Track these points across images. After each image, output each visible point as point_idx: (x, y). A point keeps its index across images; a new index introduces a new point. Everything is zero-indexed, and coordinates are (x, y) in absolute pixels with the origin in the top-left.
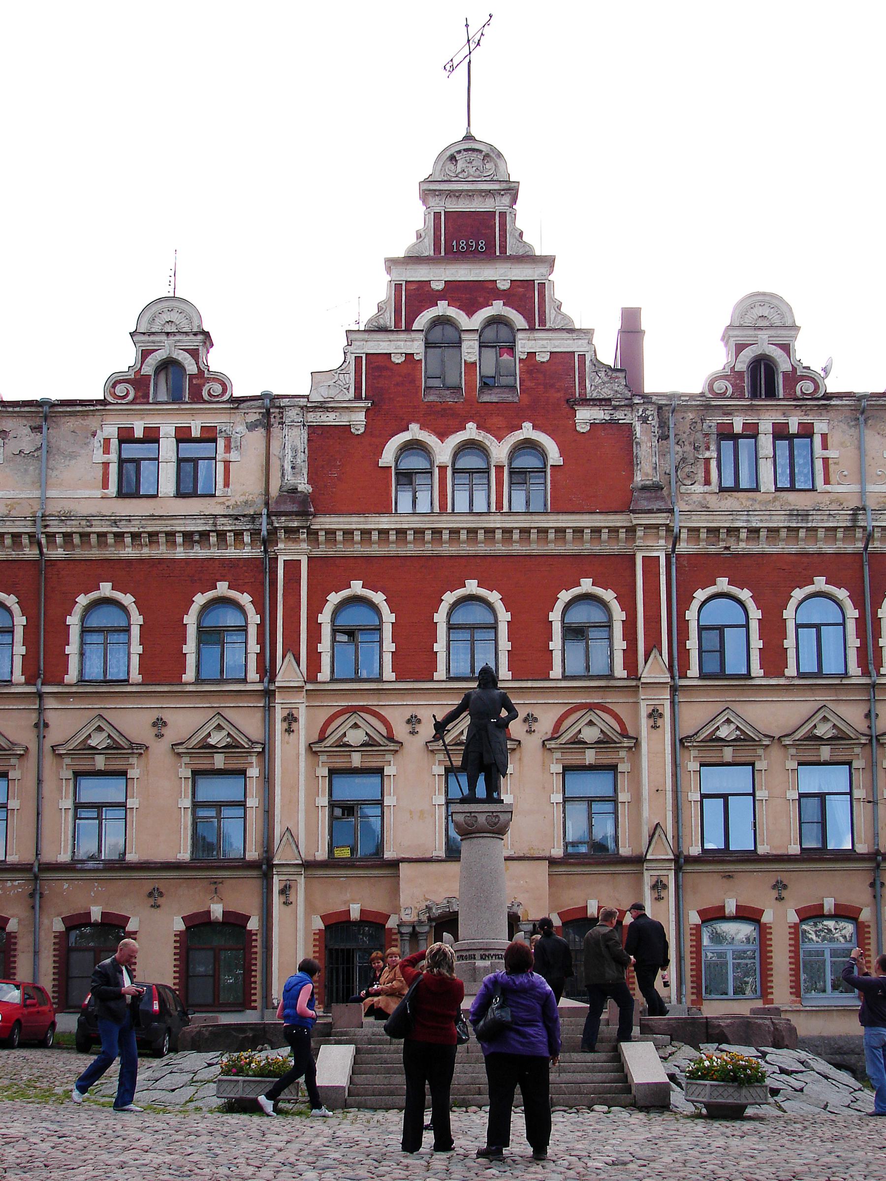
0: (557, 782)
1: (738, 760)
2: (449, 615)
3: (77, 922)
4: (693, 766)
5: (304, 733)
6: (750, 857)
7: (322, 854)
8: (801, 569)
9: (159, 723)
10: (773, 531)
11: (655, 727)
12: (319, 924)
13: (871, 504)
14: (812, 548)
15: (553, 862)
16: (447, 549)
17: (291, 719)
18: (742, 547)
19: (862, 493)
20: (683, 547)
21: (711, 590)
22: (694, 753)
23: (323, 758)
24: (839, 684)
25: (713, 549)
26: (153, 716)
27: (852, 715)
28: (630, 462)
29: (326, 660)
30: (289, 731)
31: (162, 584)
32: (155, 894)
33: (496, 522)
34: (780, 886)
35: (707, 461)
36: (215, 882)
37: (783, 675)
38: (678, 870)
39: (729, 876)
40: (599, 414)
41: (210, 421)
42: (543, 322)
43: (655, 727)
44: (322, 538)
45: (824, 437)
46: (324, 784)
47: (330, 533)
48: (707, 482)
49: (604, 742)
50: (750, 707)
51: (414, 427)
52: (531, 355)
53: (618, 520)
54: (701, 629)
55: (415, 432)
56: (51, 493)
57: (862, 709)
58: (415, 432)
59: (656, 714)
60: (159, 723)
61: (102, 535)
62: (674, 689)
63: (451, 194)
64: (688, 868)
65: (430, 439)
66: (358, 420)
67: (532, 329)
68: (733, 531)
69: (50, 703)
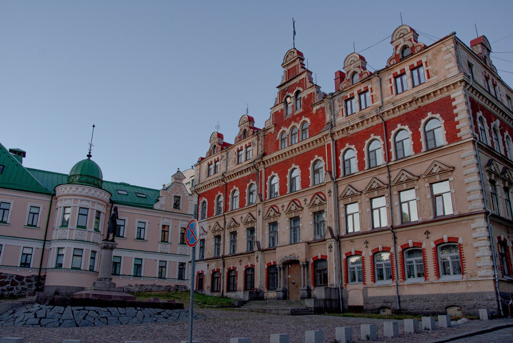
0: (312, 218)
1: (353, 201)
8: (366, 134)
10: (357, 124)
11: (330, 196)
12: (266, 267)
16: (288, 157)
17: (259, 212)
18: (351, 132)
19: (382, 102)
20: (337, 138)
23: (267, 220)
24: (379, 168)
25: (344, 136)
26: (240, 216)
27: (384, 178)
28: (324, 118)
31: (242, 184)
33: (295, 146)
35: (342, 109)
37: (363, 170)
40: (318, 107)
41: (250, 141)
42: (306, 87)
44: (266, 163)
45: (371, 89)
46: (267, 228)
47: (267, 161)
48: (343, 116)
49: (320, 204)
51: (282, 127)
52: (304, 97)
53: (320, 136)
55: (283, 129)
57: (387, 175)
58: (283, 129)
59: (330, 192)
60: (242, 218)
61: (233, 175)
63: (288, 65)
65: (285, 129)
66: (272, 130)
67: (304, 90)
68: (347, 128)
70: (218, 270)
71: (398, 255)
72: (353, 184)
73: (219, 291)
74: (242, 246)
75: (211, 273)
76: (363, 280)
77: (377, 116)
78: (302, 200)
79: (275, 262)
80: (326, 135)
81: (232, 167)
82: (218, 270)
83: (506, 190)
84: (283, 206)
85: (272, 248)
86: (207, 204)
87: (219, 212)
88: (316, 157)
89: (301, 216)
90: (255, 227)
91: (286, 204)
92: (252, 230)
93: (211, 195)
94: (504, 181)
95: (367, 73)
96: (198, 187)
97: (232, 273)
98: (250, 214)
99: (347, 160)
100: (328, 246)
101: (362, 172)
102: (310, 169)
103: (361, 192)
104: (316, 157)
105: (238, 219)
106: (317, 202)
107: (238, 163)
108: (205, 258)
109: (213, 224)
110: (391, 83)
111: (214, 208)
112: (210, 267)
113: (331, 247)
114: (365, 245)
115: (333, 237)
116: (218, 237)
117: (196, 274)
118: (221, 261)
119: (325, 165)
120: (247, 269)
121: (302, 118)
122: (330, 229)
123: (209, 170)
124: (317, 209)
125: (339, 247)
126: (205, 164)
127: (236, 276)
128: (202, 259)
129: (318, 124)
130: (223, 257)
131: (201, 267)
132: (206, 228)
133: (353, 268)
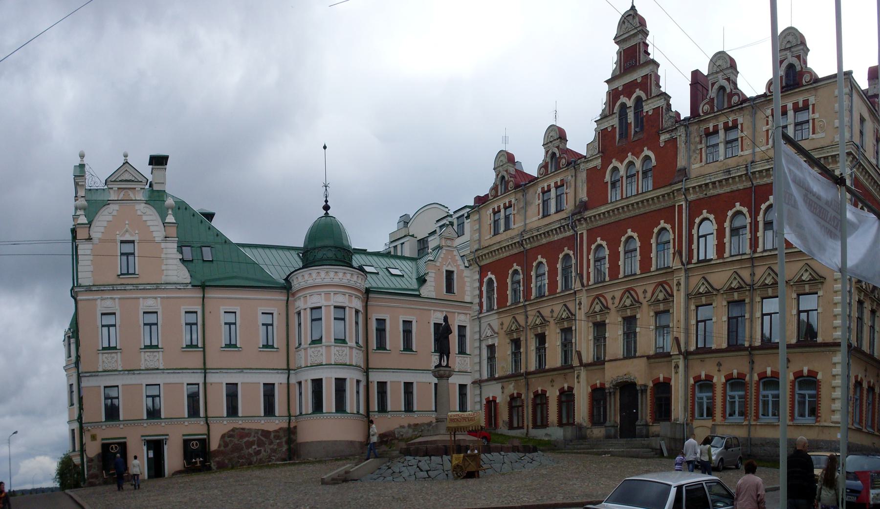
2: (625, 247)
3: (536, 395)
4: (693, 307)
5: (585, 307)
6: (710, 351)
7: (590, 360)
9: (552, 311)
12: (590, 390)
13: (757, 159)
14: (734, 188)
15: (649, 357)
17: (580, 304)
19: (754, 153)
21: (701, 217)
22: (693, 301)
29: (592, 275)
30: (580, 309)
32: (552, 381)
34: (719, 364)
36: (565, 375)
38: (685, 358)
39: (702, 360)
43: (678, 290)
46: (591, 330)
50: (712, 275)
54: (699, 237)
56: (527, 222)
60: (552, 311)
62: (686, 270)
64: (690, 357)
69: (529, 309)
70: (519, 395)
71: (754, 385)
72: (708, 277)
73: (522, 428)
74: (554, 359)
75: (509, 399)
76: (710, 413)
77: (746, 174)
78: (640, 291)
79: (602, 384)
80: (678, 190)
81: (534, 219)
82: (519, 395)
83: (873, 312)
84: (613, 298)
85: (599, 362)
86: (495, 285)
87: (516, 302)
88: (662, 224)
89: (638, 316)
90: (574, 328)
91: (618, 295)
92: (567, 332)
93: (500, 267)
94: (872, 300)
95: (738, 95)
96: (480, 253)
97: (541, 399)
98: (565, 305)
99: (702, 236)
100: (673, 365)
101: (721, 261)
102: (653, 241)
103: (718, 290)
104: (662, 224)
105: (546, 312)
106: (661, 296)
107: (544, 216)
108: (497, 376)
109: (507, 320)
110: (767, 124)
111: (508, 292)
112: (506, 391)
113: (677, 367)
114: (717, 368)
115: (680, 353)
116: (516, 343)
117: (484, 402)
118: (522, 381)
119: (674, 239)
120: (562, 392)
121: (643, 151)
122: (677, 340)
123: (496, 222)
124: (662, 307)
125: (686, 367)
126: (487, 213)
127: (547, 403)
128: (492, 378)
129: (667, 172)
130: (528, 374)
131: (494, 391)
132: (496, 325)
133: (702, 398)
